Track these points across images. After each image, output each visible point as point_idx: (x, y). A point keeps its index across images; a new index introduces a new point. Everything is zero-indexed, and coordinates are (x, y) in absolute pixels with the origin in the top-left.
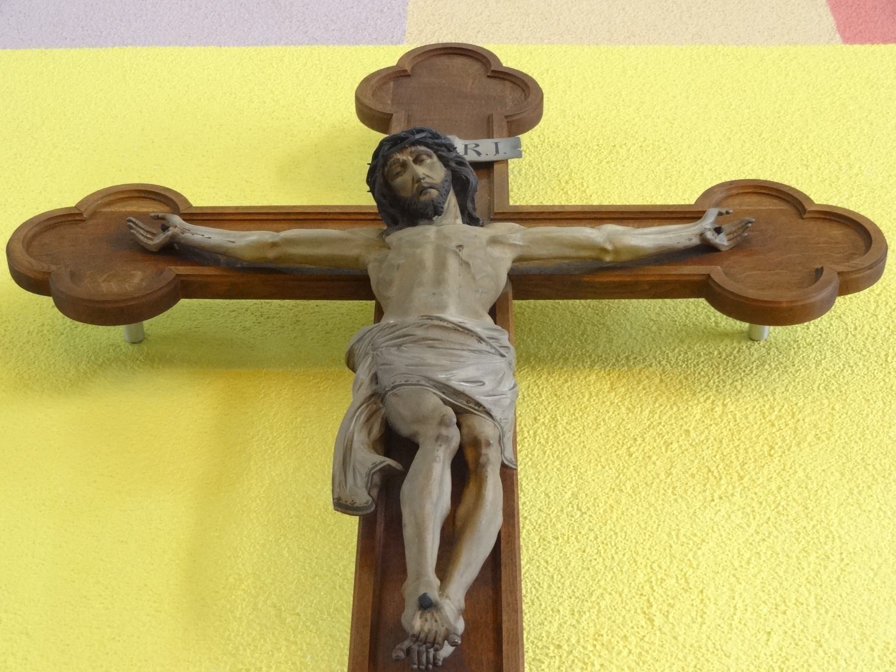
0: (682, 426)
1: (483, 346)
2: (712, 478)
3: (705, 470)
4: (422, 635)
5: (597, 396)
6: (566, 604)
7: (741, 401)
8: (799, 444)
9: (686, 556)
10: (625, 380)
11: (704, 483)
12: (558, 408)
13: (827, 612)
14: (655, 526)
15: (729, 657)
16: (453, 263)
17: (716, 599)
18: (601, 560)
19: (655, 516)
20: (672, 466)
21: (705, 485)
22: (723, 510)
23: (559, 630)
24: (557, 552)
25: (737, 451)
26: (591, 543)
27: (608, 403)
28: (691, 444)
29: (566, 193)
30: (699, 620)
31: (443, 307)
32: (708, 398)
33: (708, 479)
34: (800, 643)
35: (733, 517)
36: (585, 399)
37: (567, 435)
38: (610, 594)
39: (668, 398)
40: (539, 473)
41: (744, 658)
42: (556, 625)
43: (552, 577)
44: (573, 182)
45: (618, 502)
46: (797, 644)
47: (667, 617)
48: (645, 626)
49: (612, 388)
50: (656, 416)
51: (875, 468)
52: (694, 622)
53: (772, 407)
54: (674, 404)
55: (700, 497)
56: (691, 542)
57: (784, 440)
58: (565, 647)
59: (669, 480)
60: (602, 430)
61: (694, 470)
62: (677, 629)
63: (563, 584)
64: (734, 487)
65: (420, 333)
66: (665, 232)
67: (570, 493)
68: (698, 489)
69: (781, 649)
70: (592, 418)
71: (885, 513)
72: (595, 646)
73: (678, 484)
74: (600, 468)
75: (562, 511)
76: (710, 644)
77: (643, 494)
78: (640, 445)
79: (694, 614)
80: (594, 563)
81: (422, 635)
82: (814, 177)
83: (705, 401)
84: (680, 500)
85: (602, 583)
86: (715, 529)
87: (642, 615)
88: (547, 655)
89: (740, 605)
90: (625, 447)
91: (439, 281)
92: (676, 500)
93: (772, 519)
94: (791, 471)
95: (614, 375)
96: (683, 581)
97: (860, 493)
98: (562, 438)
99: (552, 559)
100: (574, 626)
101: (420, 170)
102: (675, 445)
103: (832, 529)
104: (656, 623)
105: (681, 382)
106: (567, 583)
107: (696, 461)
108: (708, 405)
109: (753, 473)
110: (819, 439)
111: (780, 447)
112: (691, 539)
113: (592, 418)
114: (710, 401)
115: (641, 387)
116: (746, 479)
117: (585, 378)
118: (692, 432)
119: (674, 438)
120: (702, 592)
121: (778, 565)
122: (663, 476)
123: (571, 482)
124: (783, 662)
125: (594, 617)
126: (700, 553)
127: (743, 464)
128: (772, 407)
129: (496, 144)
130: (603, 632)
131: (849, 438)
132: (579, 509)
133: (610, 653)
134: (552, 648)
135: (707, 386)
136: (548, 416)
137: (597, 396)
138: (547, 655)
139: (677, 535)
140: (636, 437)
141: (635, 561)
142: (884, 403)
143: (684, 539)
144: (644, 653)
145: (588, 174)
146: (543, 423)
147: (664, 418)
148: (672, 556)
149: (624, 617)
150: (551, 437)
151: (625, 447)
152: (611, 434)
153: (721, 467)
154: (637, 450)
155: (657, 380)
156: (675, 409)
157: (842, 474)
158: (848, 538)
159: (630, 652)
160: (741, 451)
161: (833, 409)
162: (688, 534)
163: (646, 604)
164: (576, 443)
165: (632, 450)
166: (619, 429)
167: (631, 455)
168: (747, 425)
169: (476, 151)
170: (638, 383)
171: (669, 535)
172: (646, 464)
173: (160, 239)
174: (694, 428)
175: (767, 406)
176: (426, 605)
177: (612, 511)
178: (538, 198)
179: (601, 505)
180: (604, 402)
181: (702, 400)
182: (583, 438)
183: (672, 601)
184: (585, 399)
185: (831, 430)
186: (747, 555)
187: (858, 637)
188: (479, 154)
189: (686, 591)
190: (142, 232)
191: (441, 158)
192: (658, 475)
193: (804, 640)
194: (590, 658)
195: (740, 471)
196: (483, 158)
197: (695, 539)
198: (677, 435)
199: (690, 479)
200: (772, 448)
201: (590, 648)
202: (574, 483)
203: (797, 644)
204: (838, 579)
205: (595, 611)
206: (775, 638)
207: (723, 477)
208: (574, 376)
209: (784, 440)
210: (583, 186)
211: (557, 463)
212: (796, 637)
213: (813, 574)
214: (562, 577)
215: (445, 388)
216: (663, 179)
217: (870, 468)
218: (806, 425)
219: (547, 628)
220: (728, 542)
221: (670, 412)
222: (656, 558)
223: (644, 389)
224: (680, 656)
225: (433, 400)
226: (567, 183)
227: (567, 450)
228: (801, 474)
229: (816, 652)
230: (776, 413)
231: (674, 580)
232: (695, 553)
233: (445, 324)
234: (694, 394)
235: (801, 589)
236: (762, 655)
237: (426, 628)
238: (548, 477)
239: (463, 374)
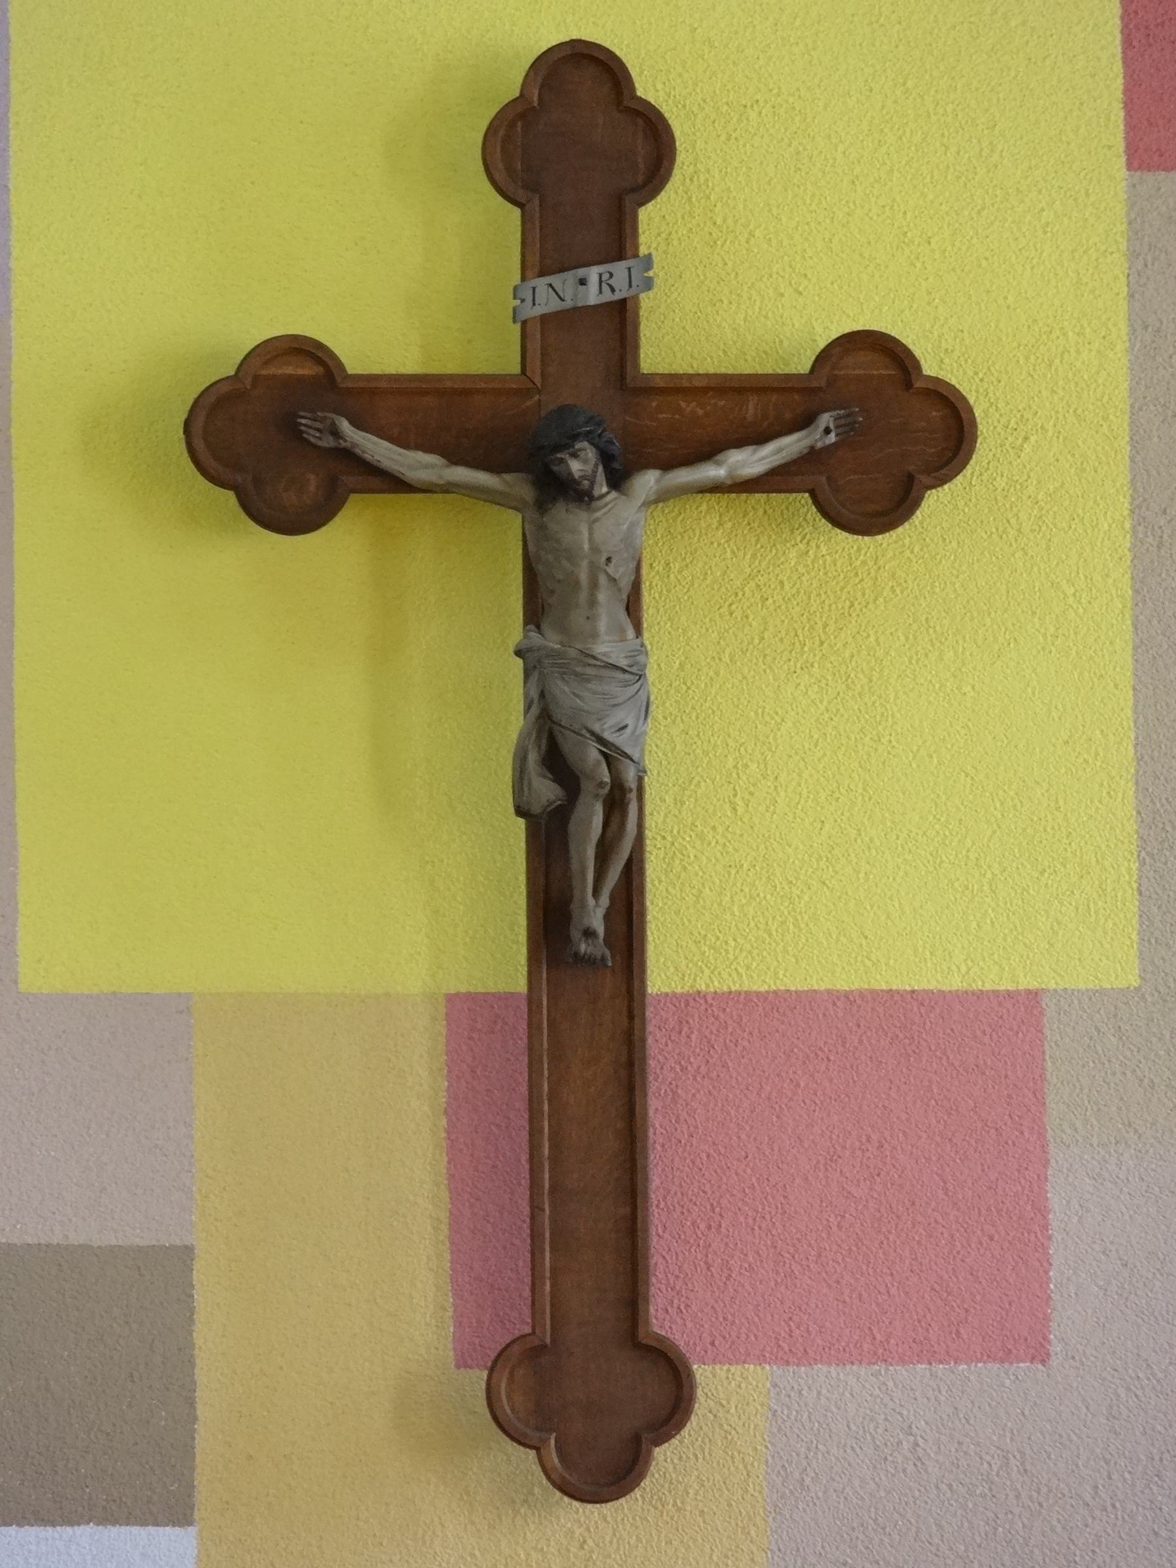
0: (778, 575)
1: (627, 676)
2: (797, 644)
3: (793, 634)
4: (586, 957)
5: (706, 534)
6: (670, 792)
7: (833, 540)
8: (876, 599)
9: (768, 737)
10: (732, 512)
11: (789, 649)
12: (671, 550)
13: (870, 799)
14: (746, 703)
15: (790, 846)
16: (603, 580)
17: (786, 787)
18: (699, 743)
19: (746, 692)
20: (765, 629)
21: (791, 652)
22: (802, 684)
23: (664, 822)
24: (665, 735)
25: (822, 608)
26: (692, 724)
27: (715, 545)
28: (783, 599)
29: (690, 199)
30: (772, 807)
31: (594, 635)
32: (804, 538)
33: (794, 644)
34: (845, 832)
35: (810, 693)
36: (696, 539)
37: (677, 588)
38: (705, 781)
39: (770, 537)
40: (653, 637)
41: (801, 847)
42: (662, 814)
43: (661, 763)
44: (698, 177)
45: (717, 674)
46: (842, 833)
47: (747, 805)
48: (729, 814)
49: (721, 524)
50: (757, 561)
51: (935, 631)
52: (767, 811)
53: (859, 550)
54: (774, 545)
55: (786, 667)
56: (773, 722)
57: (864, 594)
58: (669, 838)
59: (761, 646)
60: (708, 582)
61: (783, 632)
62: (754, 819)
63: (669, 771)
64: (815, 655)
65: (579, 669)
66: (780, 450)
67: (677, 663)
68: (784, 658)
69: (830, 837)
70: (700, 565)
71: (934, 686)
72: (691, 836)
73: (768, 651)
74: (704, 630)
75: (671, 685)
76: (778, 834)
77: (738, 663)
78: (741, 600)
79: (768, 802)
80: (694, 747)
81: (586, 957)
82: (951, 170)
83: (801, 542)
84: (768, 671)
85: (699, 769)
86: (794, 706)
87: (728, 805)
88: (655, 846)
89: (805, 792)
90: (727, 603)
91: (593, 603)
92: (765, 671)
93: (841, 694)
94: (865, 635)
95: (724, 504)
96: (762, 766)
97: (918, 661)
98: (673, 591)
99: (662, 741)
100: (676, 816)
101: (575, 467)
102: (770, 601)
103: (888, 706)
104: (739, 813)
105: (782, 513)
106: (672, 771)
107: (786, 621)
108: (802, 546)
109: (832, 637)
110: (894, 592)
111: (860, 603)
112: (773, 718)
113: (700, 565)
114: (805, 541)
115: (745, 523)
116: (826, 645)
117: (697, 508)
118: (786, 583)
119: (769, 592)
120: (776, 778)
121: (839, 748)
122: (756, 641)
123: (679, 649)
124: (830, 852)
125: (692, 806)
126: (779, 733)
127: (825, 626)
128: (859, 550)
129: (629, 269)
130: (697, 823)
131: (920, 591)
132: (685, 683)
133: (702, 843)
134: (659, 838)
135: (805, 519)
136: (662, 562)
137: (706, 534)
138: (655, 846)
139: (763, 713)
140: (738, 591)
141: (727, 745)
142: (959, 543)
143: (768, 719)
144: (727, 844)
145: (715, 163)
146: (658, 572)
147: (764, 564)
148: (756, 737)
149: (715, 806)
150: (664, 592)
151: (727, 603)
152: (716, 587)
153: (806, 628)
154: (737, 608)
155: (761, 512)
156: (774, 551)
157: (907, 639)
158: (898, 716)
159: (717, 843)
160: (826, 608)
161: (912, 552)
162: (772, 713)
163: (733, 792)
164: (686, 598)
165: (733, 607)
166: (723, 580)
167: (731, 614)
168: (835, 573)
169: (608, 284)
170: (744, 516)
171: (756, 713)
172: (744, 626)
173: (328, 442)
174: (788, 579)
175: (855, 548)
176: (589, 934)
177: (712, 686)
178: (660, 209)
179: (703, 678)
180: (712, 543)
181: (799, 538)
182: (692, 592)
183: (752, 789)
184: (696, 539)
185: (905, 581)
186: (816, 736)
187: (889, 824)
188: (613, 290)
189: (764, 778)
190: (312, 432)
191: (592, 444)
192: (753, 639)
193: (848, 827)
194: (687, 849)
195: (822, 634)
196: (618, 296)
197: (776, 718)
198: (772, 587)
199: (779, 643)
200: (852, 605)
201: (688, 839)
202: (682, 651)
203: (842, 833)
204: (884, 763)
205: (693, 800)
206: (827, 826)
207: (807, 643)
208: (687, 506)
209: (864, 594)
210: (708, 186)
211: (669, 624)
212: (842, 825)
213: (865, 757)
214: (669, 763)
215: (601, 740)
216: (792, 171)
217: (931, 631)
218: (886, 574)
219: (655, 818)
220: (803, 721)
221: (769, 557)
222: (743, 740)
223: (749, 524)
224: (754, 847)
225: (593, 753)
226: (691, 180)
227: (677, 608)
228: (872, 639)
229: (856, 840)
230: (862, 557)
231: (756, 765)
232: (776, 734)
233: (599, 663)
234: (792, 532)
235: (854, 775)
236: (815, 845)
237: (589, 951)
238: (660, 644)
239: (611, 722)
